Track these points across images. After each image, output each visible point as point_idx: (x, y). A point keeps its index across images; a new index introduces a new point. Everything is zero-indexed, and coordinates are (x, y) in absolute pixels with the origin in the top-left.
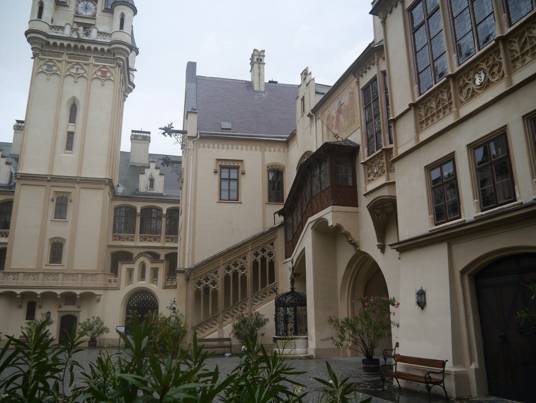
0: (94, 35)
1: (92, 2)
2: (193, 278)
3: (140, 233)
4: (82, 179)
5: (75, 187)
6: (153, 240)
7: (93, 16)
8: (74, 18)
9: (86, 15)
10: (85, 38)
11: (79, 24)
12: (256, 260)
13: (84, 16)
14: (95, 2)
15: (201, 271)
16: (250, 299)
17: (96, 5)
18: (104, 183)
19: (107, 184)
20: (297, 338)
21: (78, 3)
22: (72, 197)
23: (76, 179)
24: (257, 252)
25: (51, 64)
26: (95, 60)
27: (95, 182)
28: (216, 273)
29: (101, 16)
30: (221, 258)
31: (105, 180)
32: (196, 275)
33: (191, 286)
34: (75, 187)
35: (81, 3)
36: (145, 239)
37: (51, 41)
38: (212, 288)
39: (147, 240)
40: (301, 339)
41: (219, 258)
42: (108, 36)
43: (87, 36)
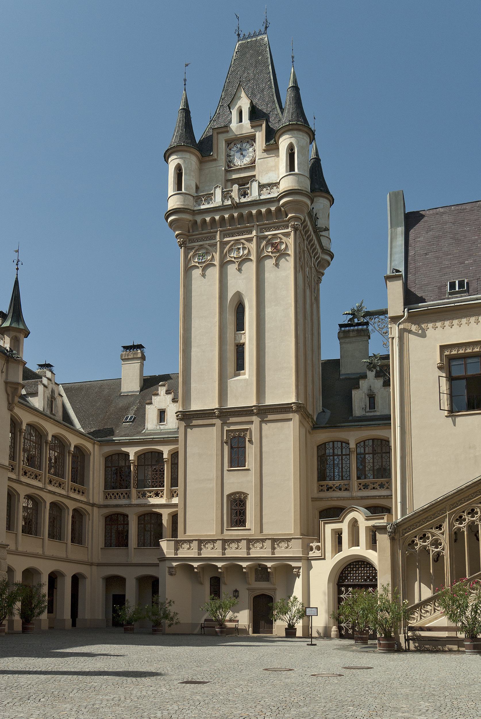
0: (254, 193)
1: (248, 142)
3: (358, 478)
6: (378, 487)
7: (252, 164)
8: (225, 175)
9: (242, 164)
10: (243, 200)
11: (234, 181)
13: (239, 167)
14: (252, 140)
17: (254, 145)
21: (229, 151)
25: (203, 251)
26: (261, 229)
29: (260, 160)
35: (233, 149)
36: (366, 487)
37: (199, 219)
39: (370, 487)
42: (275, 188)
43: (245, 197)
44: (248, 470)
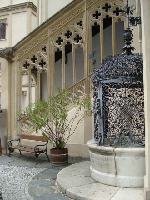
2: (18, 58)
4: (12, 7)
5: (9, 15)
12: (96, 24)
15: (27, 49)
16: (86, 80)
18: (26, 6)
19: (28, 7)
20: (121, 154)
22: (8, 22)
23: (8, 9)
24: (97, 12)
27: (21, 7)
28: (44, 49)
30: (48, 27)
31: (27, 3)
32: (21, 55)
33: (15, 68)
34: (9, 15)
38: (39, 69)
40: (130, 154)
41: (46, 29)
44: (6, 40)
